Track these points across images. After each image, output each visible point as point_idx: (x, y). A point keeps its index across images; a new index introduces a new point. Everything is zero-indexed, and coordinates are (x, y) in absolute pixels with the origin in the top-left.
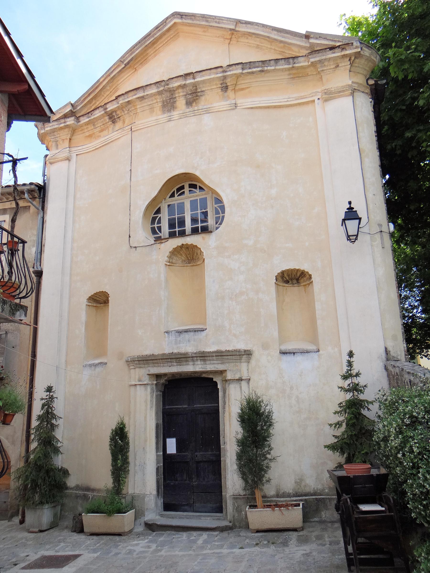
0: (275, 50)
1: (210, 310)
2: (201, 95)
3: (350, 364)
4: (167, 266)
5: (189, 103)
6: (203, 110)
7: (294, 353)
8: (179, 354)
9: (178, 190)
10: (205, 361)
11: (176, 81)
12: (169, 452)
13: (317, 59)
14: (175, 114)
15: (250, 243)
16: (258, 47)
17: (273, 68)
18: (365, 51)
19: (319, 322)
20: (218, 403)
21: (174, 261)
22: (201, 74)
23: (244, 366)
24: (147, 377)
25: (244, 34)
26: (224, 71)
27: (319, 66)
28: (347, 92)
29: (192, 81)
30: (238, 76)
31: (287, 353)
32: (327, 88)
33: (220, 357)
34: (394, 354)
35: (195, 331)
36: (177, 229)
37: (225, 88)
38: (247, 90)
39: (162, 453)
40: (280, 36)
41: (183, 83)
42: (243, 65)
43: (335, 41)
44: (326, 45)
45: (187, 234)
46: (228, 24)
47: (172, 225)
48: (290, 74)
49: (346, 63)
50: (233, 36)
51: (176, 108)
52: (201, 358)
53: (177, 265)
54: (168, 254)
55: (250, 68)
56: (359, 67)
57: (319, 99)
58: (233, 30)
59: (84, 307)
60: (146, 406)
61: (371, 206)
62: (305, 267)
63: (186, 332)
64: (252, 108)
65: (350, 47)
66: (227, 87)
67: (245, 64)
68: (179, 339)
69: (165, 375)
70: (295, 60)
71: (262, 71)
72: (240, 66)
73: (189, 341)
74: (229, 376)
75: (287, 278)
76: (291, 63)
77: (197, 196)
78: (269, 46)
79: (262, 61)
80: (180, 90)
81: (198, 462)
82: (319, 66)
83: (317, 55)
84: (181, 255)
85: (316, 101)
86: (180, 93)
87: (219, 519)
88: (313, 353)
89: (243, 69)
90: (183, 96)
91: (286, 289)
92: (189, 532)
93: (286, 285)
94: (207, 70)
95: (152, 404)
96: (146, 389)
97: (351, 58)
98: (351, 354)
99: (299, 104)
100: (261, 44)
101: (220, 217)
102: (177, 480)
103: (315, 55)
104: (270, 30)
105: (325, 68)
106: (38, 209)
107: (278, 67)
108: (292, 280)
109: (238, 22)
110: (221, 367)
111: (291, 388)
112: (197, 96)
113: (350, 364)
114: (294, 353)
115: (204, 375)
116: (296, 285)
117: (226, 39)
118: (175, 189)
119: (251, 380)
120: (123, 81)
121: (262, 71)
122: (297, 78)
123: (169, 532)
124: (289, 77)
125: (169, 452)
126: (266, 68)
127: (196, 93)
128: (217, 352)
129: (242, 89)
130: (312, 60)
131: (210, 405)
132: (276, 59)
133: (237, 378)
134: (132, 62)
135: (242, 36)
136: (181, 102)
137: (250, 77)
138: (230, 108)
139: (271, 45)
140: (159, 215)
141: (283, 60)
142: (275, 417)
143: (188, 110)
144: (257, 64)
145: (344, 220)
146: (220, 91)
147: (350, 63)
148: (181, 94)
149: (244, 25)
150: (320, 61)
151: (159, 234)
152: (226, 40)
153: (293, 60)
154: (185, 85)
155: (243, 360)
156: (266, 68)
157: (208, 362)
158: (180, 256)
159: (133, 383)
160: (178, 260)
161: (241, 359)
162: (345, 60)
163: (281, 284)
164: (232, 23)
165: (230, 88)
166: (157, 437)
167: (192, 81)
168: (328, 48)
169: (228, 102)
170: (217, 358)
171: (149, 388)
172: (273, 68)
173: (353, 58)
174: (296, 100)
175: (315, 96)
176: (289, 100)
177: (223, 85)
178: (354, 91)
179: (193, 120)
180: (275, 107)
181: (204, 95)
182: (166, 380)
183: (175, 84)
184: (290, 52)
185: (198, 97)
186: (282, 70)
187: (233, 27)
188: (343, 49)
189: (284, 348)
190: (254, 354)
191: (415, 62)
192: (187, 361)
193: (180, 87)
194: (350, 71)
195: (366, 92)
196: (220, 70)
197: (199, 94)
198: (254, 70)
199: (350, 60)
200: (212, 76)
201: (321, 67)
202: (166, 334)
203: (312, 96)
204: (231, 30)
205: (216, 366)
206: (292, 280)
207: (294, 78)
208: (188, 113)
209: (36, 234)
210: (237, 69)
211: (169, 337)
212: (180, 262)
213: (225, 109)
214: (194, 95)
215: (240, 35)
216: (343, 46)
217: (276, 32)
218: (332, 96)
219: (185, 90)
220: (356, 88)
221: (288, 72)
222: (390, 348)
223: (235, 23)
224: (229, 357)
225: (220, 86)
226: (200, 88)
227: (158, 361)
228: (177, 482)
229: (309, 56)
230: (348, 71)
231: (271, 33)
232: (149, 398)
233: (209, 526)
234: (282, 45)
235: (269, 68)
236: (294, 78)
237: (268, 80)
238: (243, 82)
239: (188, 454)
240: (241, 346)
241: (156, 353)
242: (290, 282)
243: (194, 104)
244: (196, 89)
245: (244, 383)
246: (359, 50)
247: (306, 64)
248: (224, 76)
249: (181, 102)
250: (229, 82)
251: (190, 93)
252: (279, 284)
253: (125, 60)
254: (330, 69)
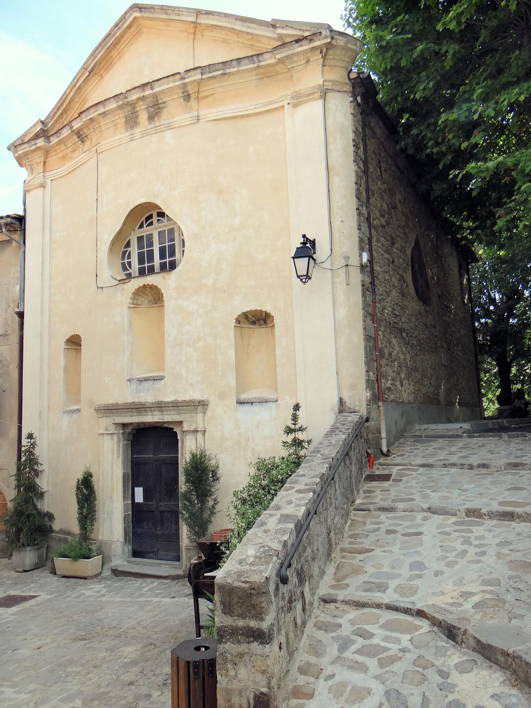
0: (242, 43)
1: (169, 357)
2: (163, 107)
3: (295, 418)
4: (132, 309)
5: (151, 118)
6: (164, 126)
7: (252, 403)
8: (140, 404)
9: (147, 219)
10: (162, 411)
11: (134, 93)
12: (136, 501)
13: (283, 55)
14: (137, 131)
15: (210, 282)
16: (224, 41)
17: (235, 69)
18: (339, 40)
19: (279, 369)
20: (177, 453)
21: (139, 302)
22: (159, 83)
23: (200, 416)
24: (113, 426)
25: (208, 27)
26: (183, 78)
27: (287, 62)
28: (316, 95)
29: (150, 92)
30: (199, 83)
31: (244, 403)
32: (297, 90)
33: (175, 408)
34: (350, 405)
35: (154, 380)
36: (146, 265)
37: (187, 97)
38: (211, 98)
39: (130, 502)
40: (246, 27)
41: (142, 95)
42: (201, 70)
43: (303, 30)
44: (294, 35)
45: (156, 271)
46: (189, 16)
47: (141, 261)
48: (257, 74)
49: (317, 58)
50: (197, 29)
51: (138, 124)
52: (159, 409)
53: (143, 306)
54: (130, 295)
55: (210, 72)
56: (334, 59)
57: (288, 104)
58: (194, 22)
59: (62, 350)
60: (113, 456)
61: (336, 236)
62: (267, 308)
63: (146, 380)
64: (216, 120)
65: (318, 37)
66: (189, 96)
67: (204, 68)
68: (139, 388)
69: (131, 424)
70: (260, 58)
71: (224, 74)
72: (199, 71)
73: (148, 390)
74: (186, 427)
75: (254, 319)
76: (256, 62)
77: (164, 226)
78: (236, 40)
79: (222, 63)
80: (141, 103)
81: (162, 512)
82: (287, 62)
83: (283, 50)
84: (147, 295)
85: (286, 106)
86: (141, 107)
87: (175, 568)
88: (271, 403)
89: (202, 74)
90: (145, 109)
91: (253, 331)
92: (145, 579)
93: (253, 326)
94: (164, 78)
95: (119, 453)
96: (112, 439)
97: (322, 50)
98: (297, 407)
99: (269, 111)
100: (227, 38)
101: (169, 257)
102: (144, 529)
103: (280, 51)
104: (233, 20)
105: (295, 65)
106: (19, 243)
107: (241, 68)
108: (258, 320)
109: (199, 12)
110: (177, 418)
111: (248, 440)
112: (159, 108)
113: (295, 418)
114: (252, 403)
115: (165, 425)
116: (263, 326)
117: (190, 33)
118: (144, 219)
119: (207, 431)
120: (90, 91)
121: (224, 74)
122: (267, 79)
123: (128, 578)
124: (257, 77)
125: (136, 501)
126: (228, 71)
127: (158, 105)
128: (172, 402)
129: (206, 97)
130: (278, 56)
131: (173, 455)
132: (238, 59)
133: (192, 430)
134: (95, 68)
135: (206, 29)
136: (143, 117)
137: (212, 81)
138: (192, 122)
139: (238, 37)
140: (129, 249)
141: (246, 59)
142: (221, 472)
143: (150, 127)
144: (217, 67)
145: (294, 258)
146: (182, 100)
147: (322, 56)
148: (143, 107)
149: (205, 16)
150: (287, 57)
152: (190, 35)
153: (258, 58)
154: (143, 97)
155: (198, 411)
156: (228, 71)
157: (165, 413)
158: (146, 296)
159: (102, 431)
160: (144, 300)
161: (196, 410)
162: (316, 53)
163: (246, 326)
164: (192, 14)
165: (193, 97)
166: (125, 486)
167: (150, 92)
168: (294, 41)
169: (190, 115)
170: (173, 408)
171: (115, 437)
172: (235, 69)
173: (324, 50)
174: (265, 106)
175: (284, 100)
176: (257, 106)
177: (185, 94)
178: (324, 94)
179: (155, 138)
180: (242, 116)
181: (166, 106)
182: (132, 429)
183: (134, 97)
184: (259, 45)
185: (160, 110)
186: (247, 70)
187: (193, 19)
188: (311, 40)
189: (244, 397)
190: (210, 405)
191: (403, 46)
192: (146, 411)
193: (139, 99)
194: (324, 66)
195: (346, 90)
196: (178, 77)
197: (161, 106)
198: (215, 74)
199: (321, 52)
200: (171, 85)
201: (291, 63)
202: (129, 383)
203: (282, 101)
204: (193, 22)
205: (173, 417)
206: (258, 320)
207: (263, 78)
208: (150, 130)
209: (19, 270)
210: (195, 75)
211: (131, 386)
212: (146, 302)
213: (187, 123)
214: (156, 107)
215: (204, 28)
216: (310, 37)
217: (240, 23)
218: (302, 99)
219: (145, 102)
220: (329, 87)
221: (254, 72)
222: (346, 399)
223: (195, 15)
224: (185, 408)
225: (181, 95)
226: (161, 99)
227: (121, 410)
228: (144, 531)
229: (274, 52)
230: (321, 66)
231: (235, 24)
232: (115, 448)
233: (162, 574)
234: (250, 36)
235: (232, 70)
236: (263, 78)
237: (234, 84)
238: (205, 88)
239: (153, 503)
240: (197, 396)
241: (120, 403)
242: (257, 323)
243: (156, 119)
244: (157, 101)
245: (199, 435)
246: (329, 40)
247: (273, 61)
248: (183, 84)
249: (143, 117)
250: (191, 90)
251: (151, 105)
252: (243, 326)
253: (88, 67)
254: (300, 65)
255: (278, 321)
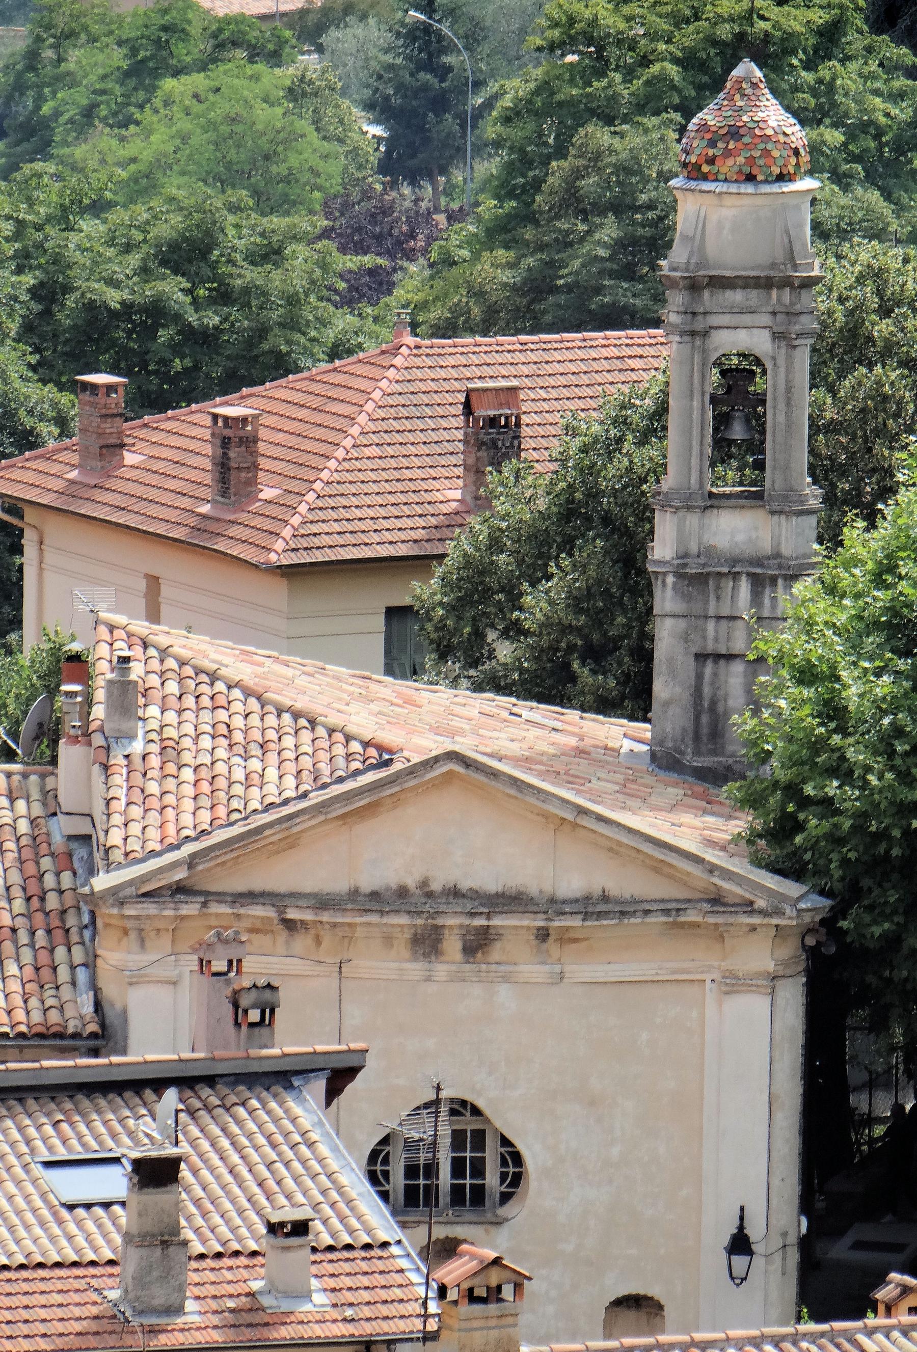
14: (441, 970)
15: (569, 1248)
51: (442, 954)
61: (774, 1202)
62: (654, 1291)
85: (708, 982)
89: (584, 920)
138: (549, 981)
140: (387, 1149)
151: (382, 1185)
179: (477, 990)
197: (491, 937)
203: (702, 972)
243: (479, 955)
249: (453, 946)
255: (667, 1311)
